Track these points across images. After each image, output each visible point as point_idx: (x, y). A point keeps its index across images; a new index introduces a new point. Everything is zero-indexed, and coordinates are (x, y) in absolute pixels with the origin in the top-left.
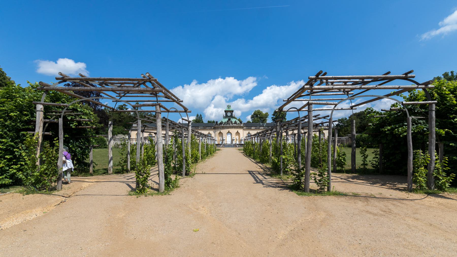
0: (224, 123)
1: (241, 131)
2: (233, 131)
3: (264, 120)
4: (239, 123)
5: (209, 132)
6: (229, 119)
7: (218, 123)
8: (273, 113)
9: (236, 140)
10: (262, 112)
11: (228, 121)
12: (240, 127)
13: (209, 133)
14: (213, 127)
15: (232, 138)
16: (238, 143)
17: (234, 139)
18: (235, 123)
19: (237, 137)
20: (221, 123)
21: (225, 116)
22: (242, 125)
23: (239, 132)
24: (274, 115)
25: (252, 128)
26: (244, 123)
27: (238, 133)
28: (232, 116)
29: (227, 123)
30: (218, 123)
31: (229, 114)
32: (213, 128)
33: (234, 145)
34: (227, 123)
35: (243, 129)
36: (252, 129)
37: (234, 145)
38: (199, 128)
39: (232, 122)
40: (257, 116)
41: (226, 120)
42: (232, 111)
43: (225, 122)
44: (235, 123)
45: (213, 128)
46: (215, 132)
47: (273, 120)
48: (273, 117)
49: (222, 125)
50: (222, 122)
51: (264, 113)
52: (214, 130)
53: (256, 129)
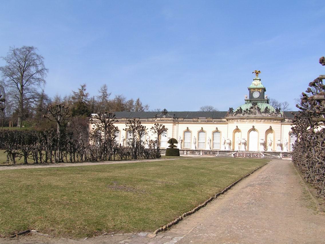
0: (245, 111)
2: (262, 126)
4: (273, 112)
6: (255, 104)
7: (235, 111)
11: (252, 108)
18: (267, 110)
20: (240, 111)
21: (248, 98)
22: (279, 116)
28: (262, 99)
29: (249, 111)
30: (235, 111)
31: (256, 95)
34: (249, 111)
38: (199, 121)
39: (259, 109)
41: (250, 105)
42: (264, 90)
43: (247, 109)
44: (267, 110)
49: (241, 115)
50: (241, 109)
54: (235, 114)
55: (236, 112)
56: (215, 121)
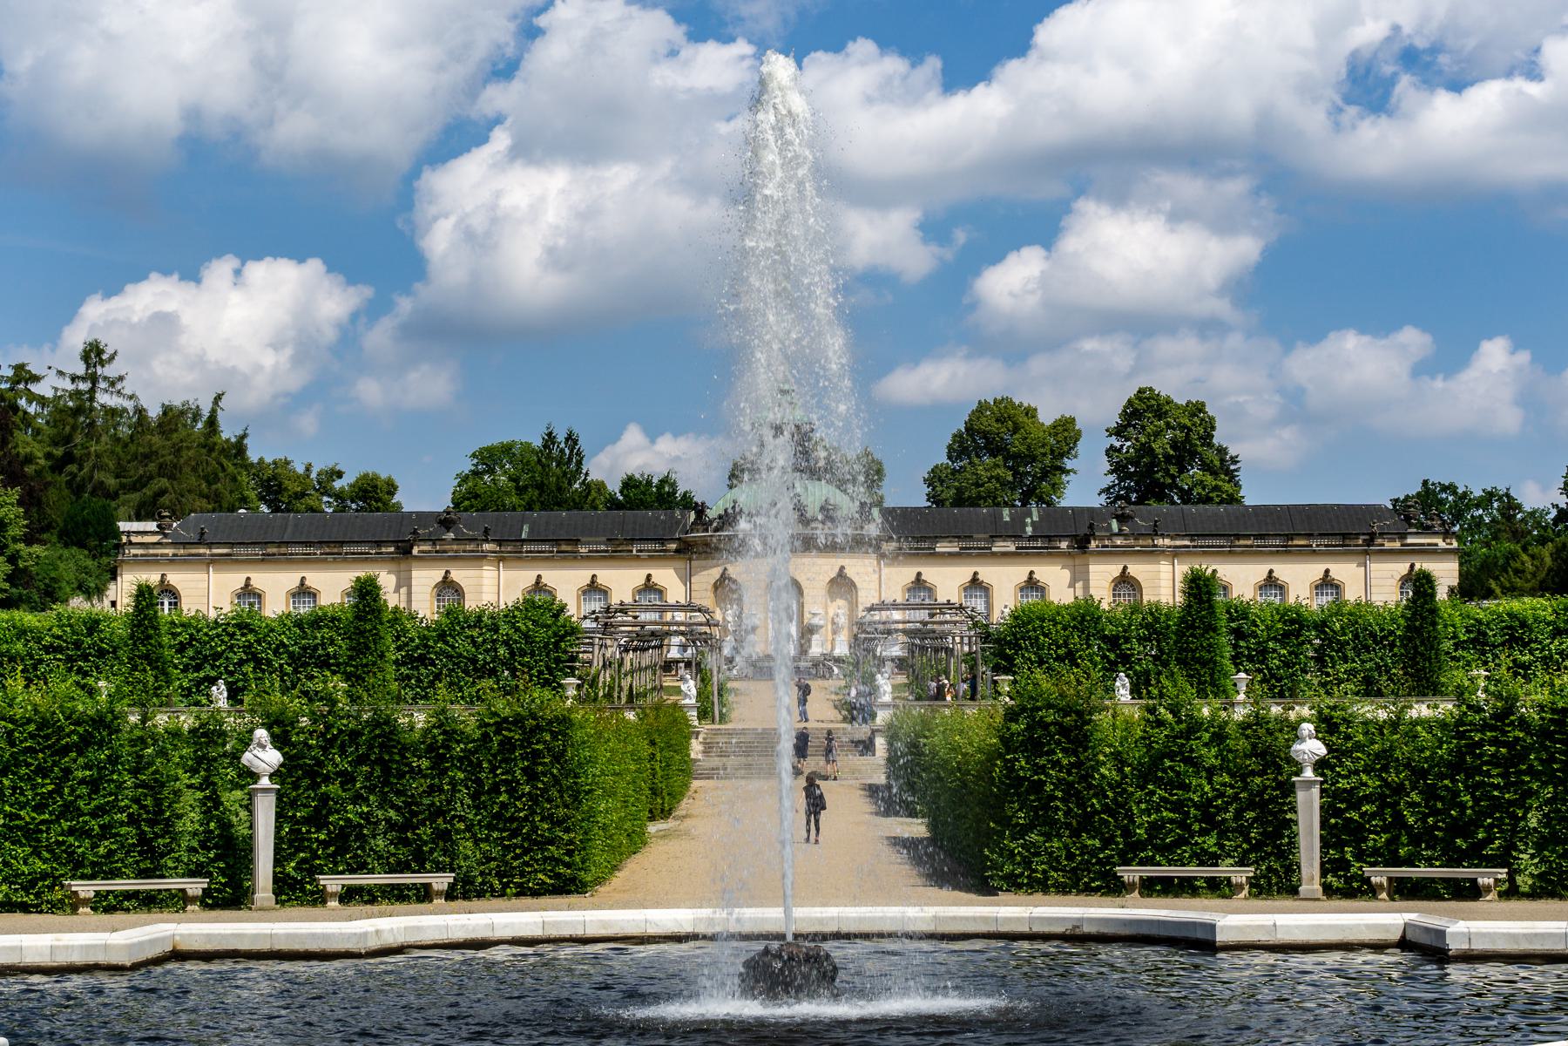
1: (861, 568)
3: (1045, 474)
5: (649, 577)
7: (712, 513)
8: (1114, 420)
9: (834, 632)
10: (1030, 413)
12: (858, 544)
13: (649, 587)
14: (673, 540)
15: (807, 616)
16: (842, 650)
17: (816, 621)
19: (839, 608)
23: (849, 572)
24: (1119, 432)
25: (942, 547)
26: (888, 513)
27: (842, 584)
32: (673, 546)
33: (816, 665)
35: (882, 556)
36: (942, 555)
37: (816, 665)
38: (583, 550)
40: (994, 447)
45: (673, 546)
46: (686, 579)
47: (1118, 469)
48: (1117, 444)
51: (1047, 417)
52: (680, 564)
53: (969, 555)
54: (715, 524)
55: (720, 517)
56: (641, 551)
